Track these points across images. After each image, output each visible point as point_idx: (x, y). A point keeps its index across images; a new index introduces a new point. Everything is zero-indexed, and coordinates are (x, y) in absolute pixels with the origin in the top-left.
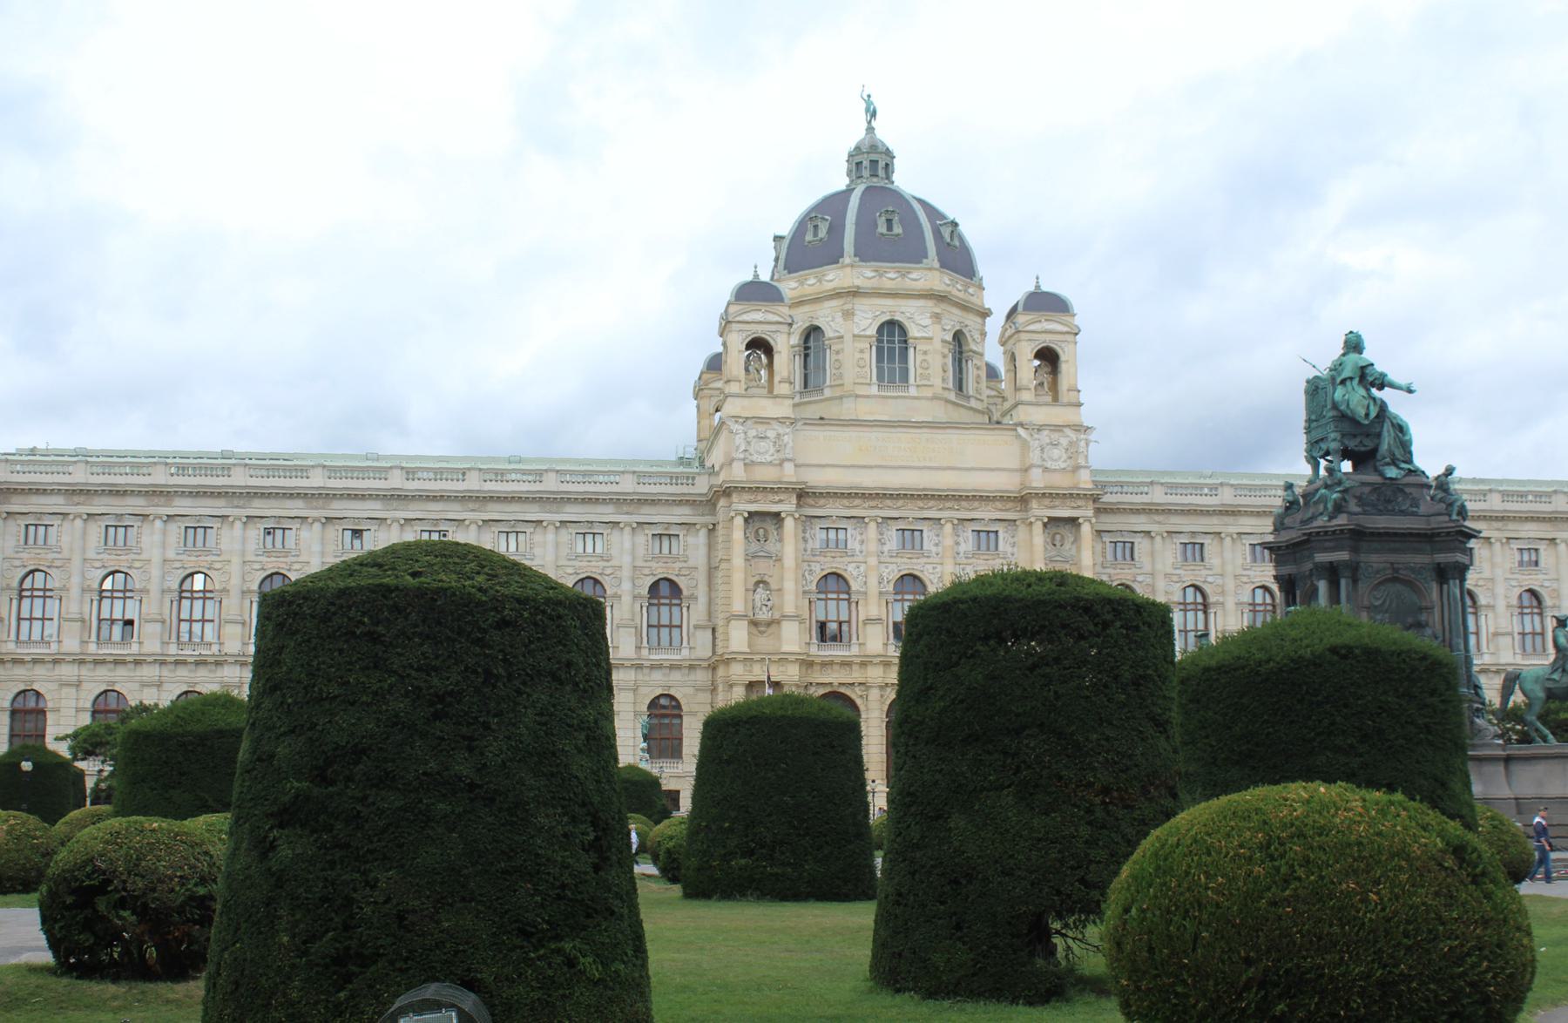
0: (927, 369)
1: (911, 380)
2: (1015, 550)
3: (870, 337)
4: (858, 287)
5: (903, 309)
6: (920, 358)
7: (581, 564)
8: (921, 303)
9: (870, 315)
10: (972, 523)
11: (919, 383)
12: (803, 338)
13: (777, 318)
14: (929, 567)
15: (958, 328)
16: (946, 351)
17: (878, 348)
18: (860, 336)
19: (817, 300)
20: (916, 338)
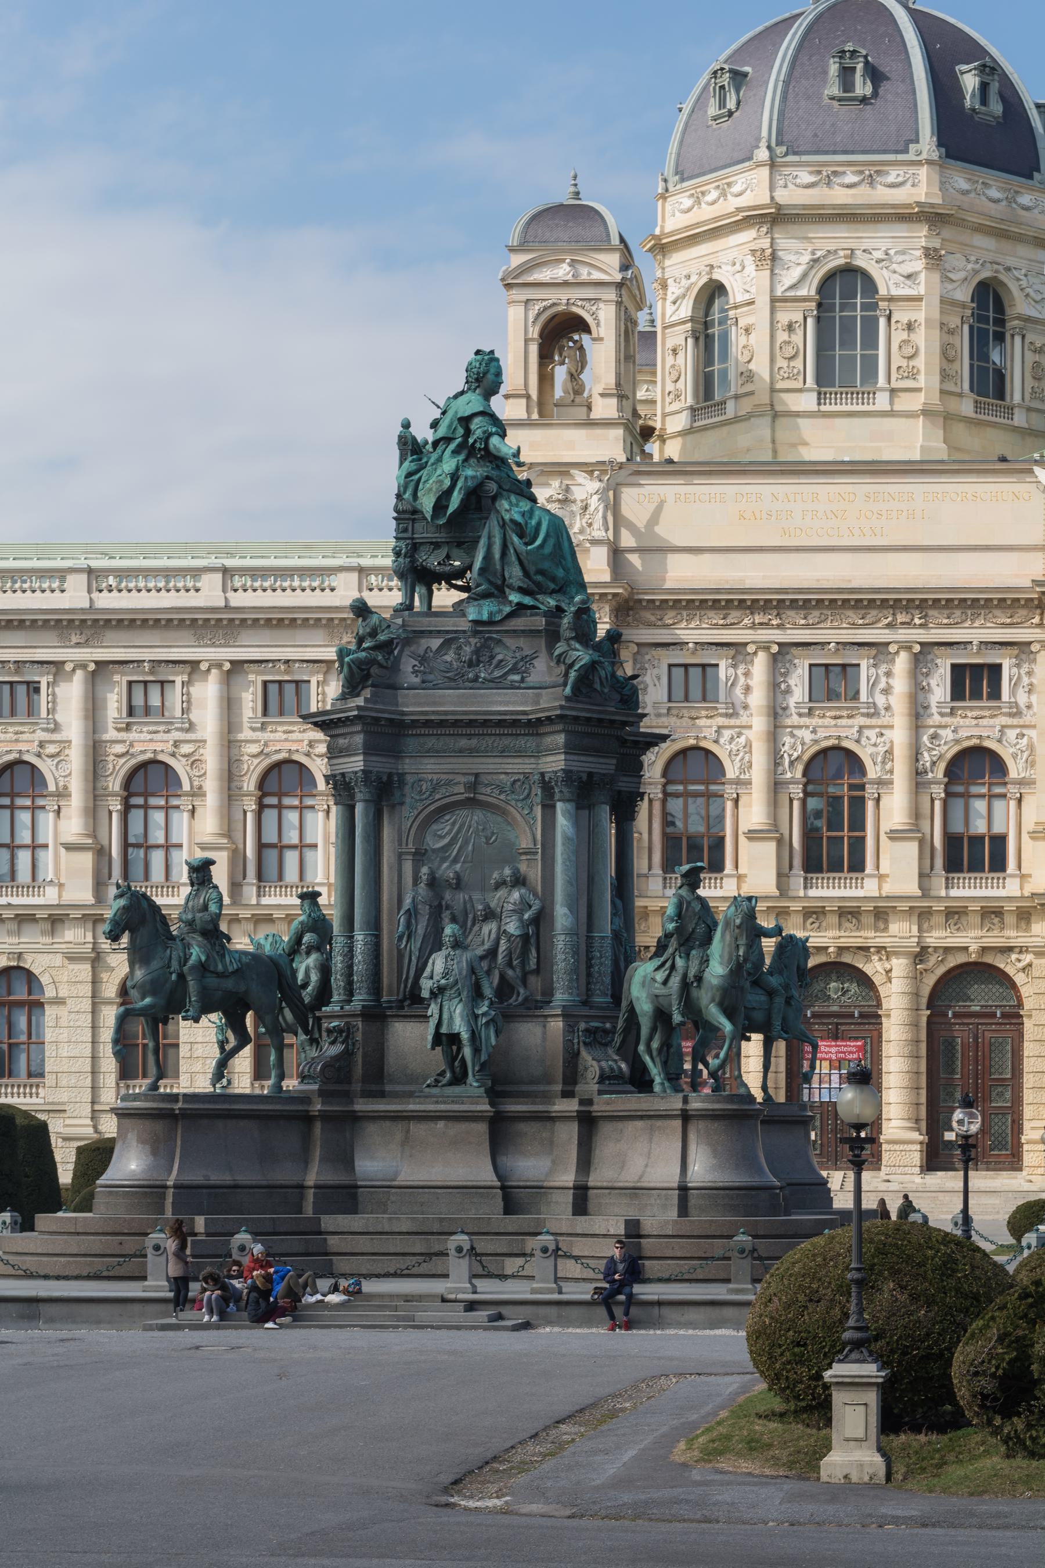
0: (910, 358)
1: (882, 381)
2: (1034, 698)
3: (804, 299)
4: (779, 207)
5: (867, 244)
6: (899, 336)
7: (272, 736)
8: (901, 230)
9: (806, 258)
10: (949, 650)
11: (894, 384)
12: (703, 306)
13: (597, 276)
14: (872, 733)
15: (986, 274)
16: (954, 321)
17: (818, 319)
18: (785, 300)
19: (716, 232)
20: (891, 299)
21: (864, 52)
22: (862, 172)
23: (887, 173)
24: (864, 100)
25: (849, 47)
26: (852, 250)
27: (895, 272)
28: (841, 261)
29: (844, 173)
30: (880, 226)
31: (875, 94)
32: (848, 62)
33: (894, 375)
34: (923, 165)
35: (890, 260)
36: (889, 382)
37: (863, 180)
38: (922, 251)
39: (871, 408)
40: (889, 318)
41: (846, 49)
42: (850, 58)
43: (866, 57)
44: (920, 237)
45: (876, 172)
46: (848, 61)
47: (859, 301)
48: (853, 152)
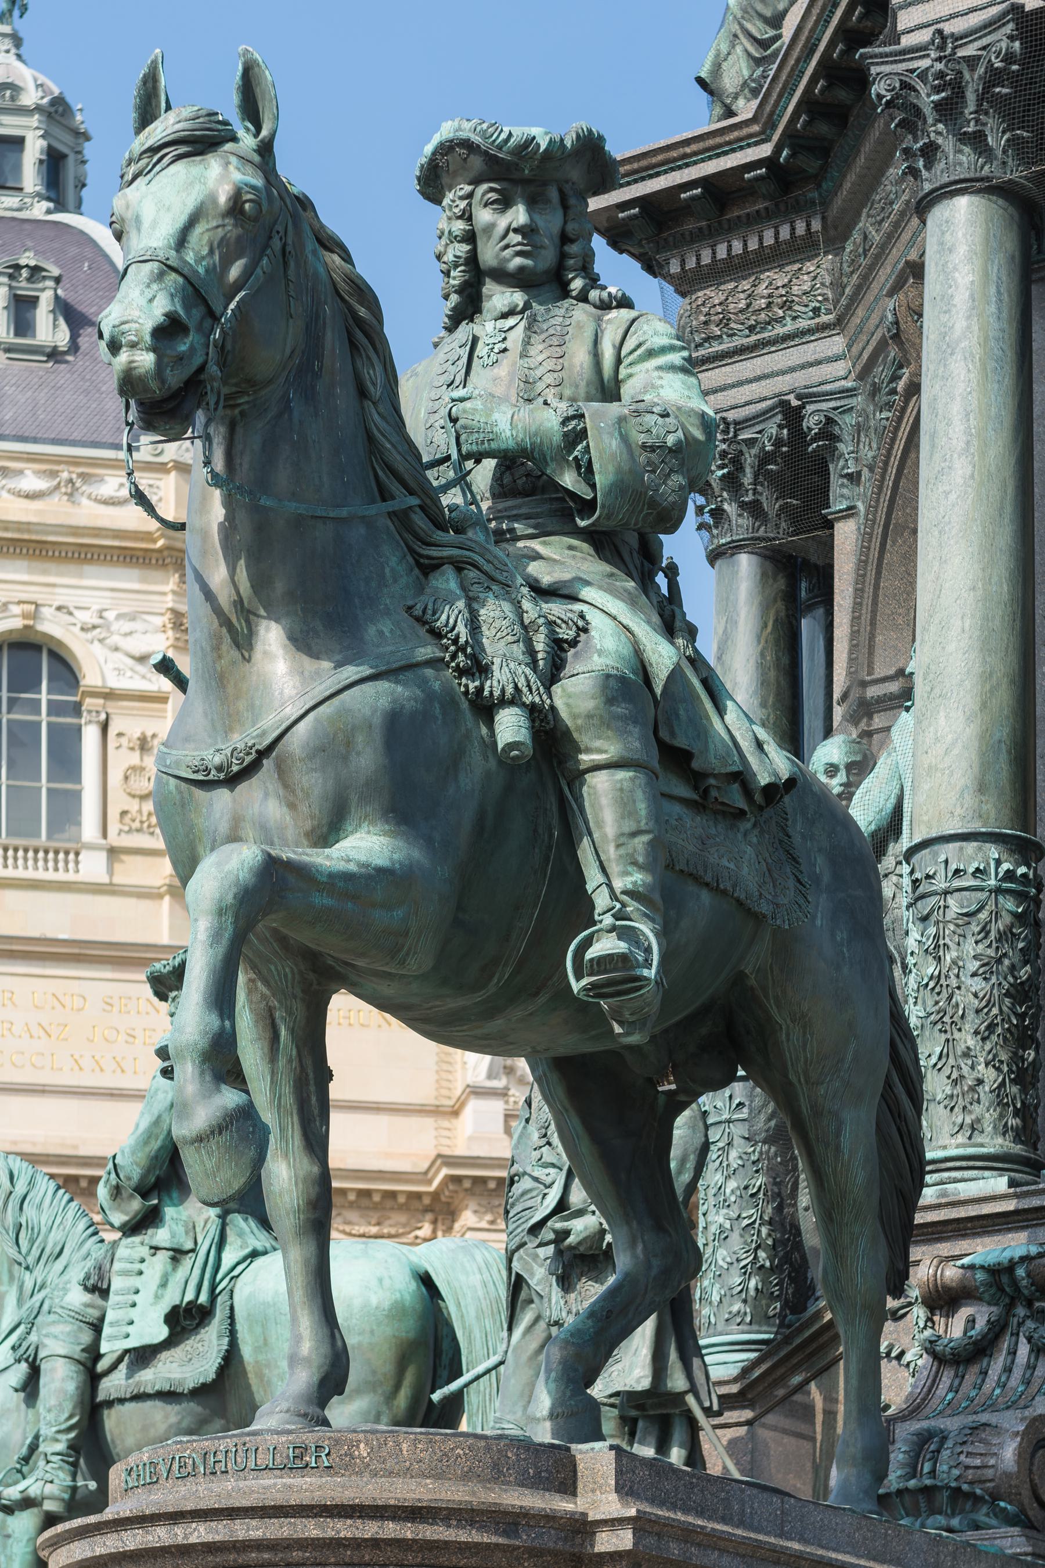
5: (62, 597)
8: (128, 579)
11: (114, 839)
20: (110, 695)
21: (56, 272)
22: (53, 474)
23: (101, 480)
24: (54, 355)
25: (28, 259)
26: (37, 605)
27: (116, 649)
28: (17, 623)
29: (21, 472)
30: (88, 569)
31: (74, 347)
32: (24, 287)
33: (113, 827)
34: (168, 472)
35: (107, 626)
36: (105, 835)
37: (57, 487)
38: (169, 615)
39: (71, 877)
40: (105, 727)
41: (23, 262)
42: (29, 280)
43: (58, 280)
44: (164, 594)
45: (81, 475)
46: (24, 284)
47: (44, 697)
48: (35, 440)
